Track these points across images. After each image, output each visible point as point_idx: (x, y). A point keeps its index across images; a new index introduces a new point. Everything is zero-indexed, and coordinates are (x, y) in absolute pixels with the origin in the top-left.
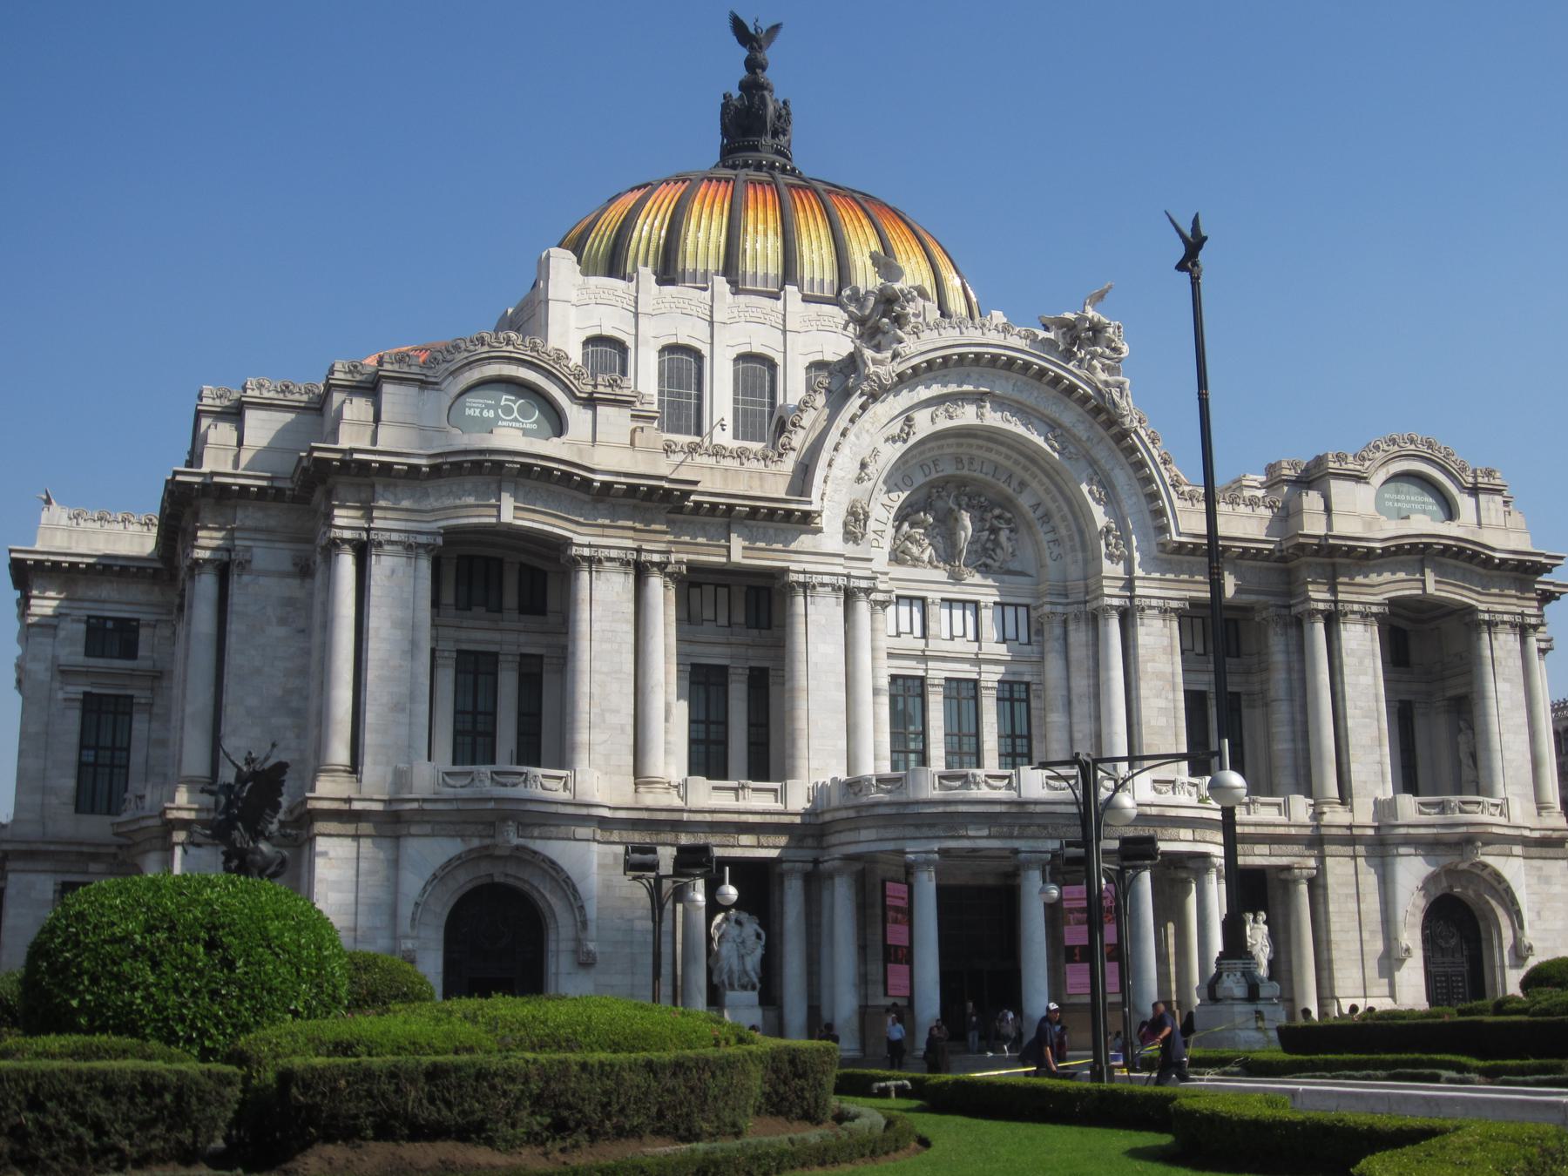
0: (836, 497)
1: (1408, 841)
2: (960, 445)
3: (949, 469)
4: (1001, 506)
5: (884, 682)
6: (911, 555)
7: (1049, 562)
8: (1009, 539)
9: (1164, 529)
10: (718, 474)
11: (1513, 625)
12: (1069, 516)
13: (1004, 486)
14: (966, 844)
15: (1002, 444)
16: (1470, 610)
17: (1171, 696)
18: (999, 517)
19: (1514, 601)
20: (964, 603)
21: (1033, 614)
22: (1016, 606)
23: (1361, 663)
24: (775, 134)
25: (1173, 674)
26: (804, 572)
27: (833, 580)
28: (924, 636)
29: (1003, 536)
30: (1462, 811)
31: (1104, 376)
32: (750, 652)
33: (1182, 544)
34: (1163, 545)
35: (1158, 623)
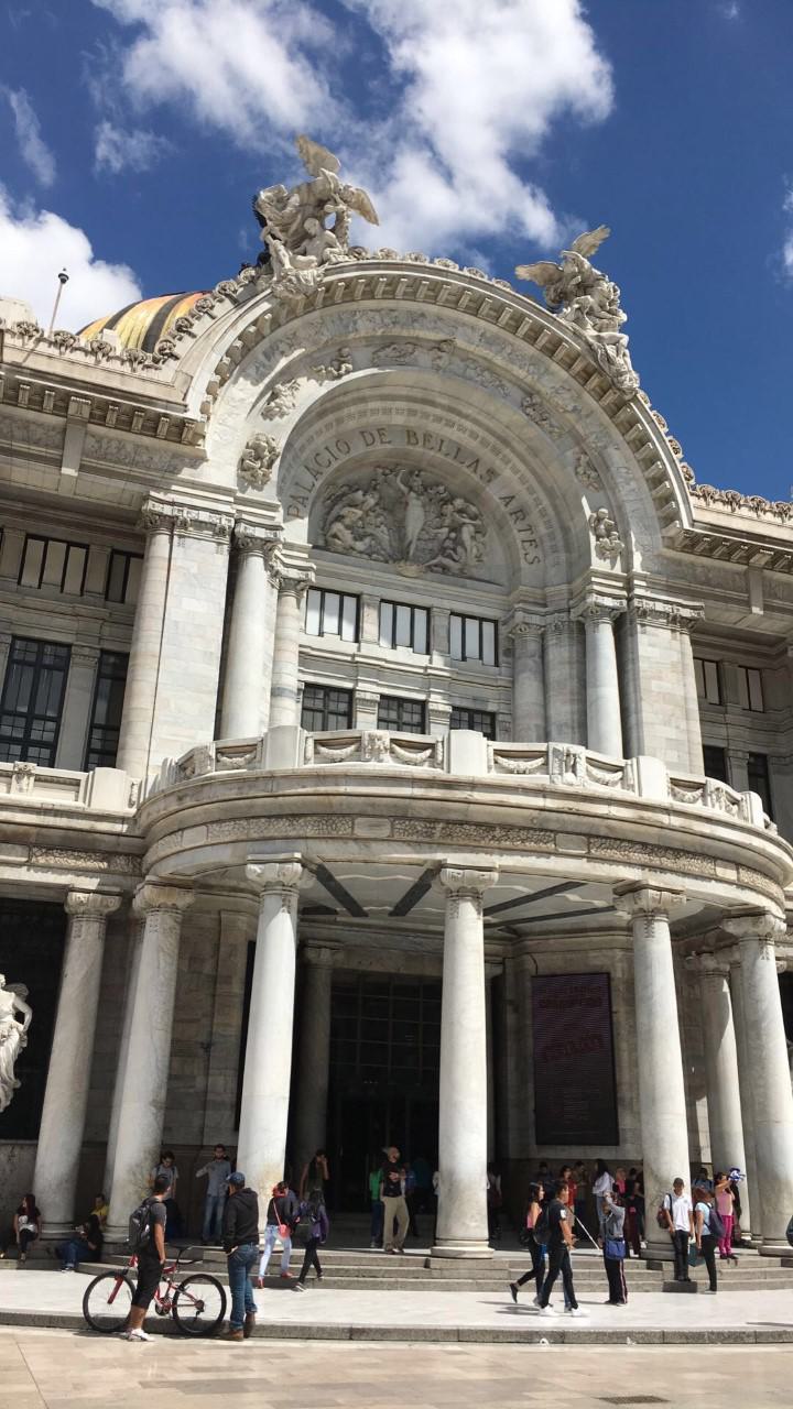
0: (230, 421)
2: (412, 413)
4: (466, 501)
5: (292, 678)
7: (523, 564)
8: (473, 538)
9: (675, 516)
12: (551, 511)
15: (466, 417)
17: (683, 725)
18: (460, 511)
21: (503, 630)
22: (482, 620)
25: (686, 699)
26: (172, 504)
27: (215, 519)
28: (357, 640)
29: (467, 533)
32: (107, 630)
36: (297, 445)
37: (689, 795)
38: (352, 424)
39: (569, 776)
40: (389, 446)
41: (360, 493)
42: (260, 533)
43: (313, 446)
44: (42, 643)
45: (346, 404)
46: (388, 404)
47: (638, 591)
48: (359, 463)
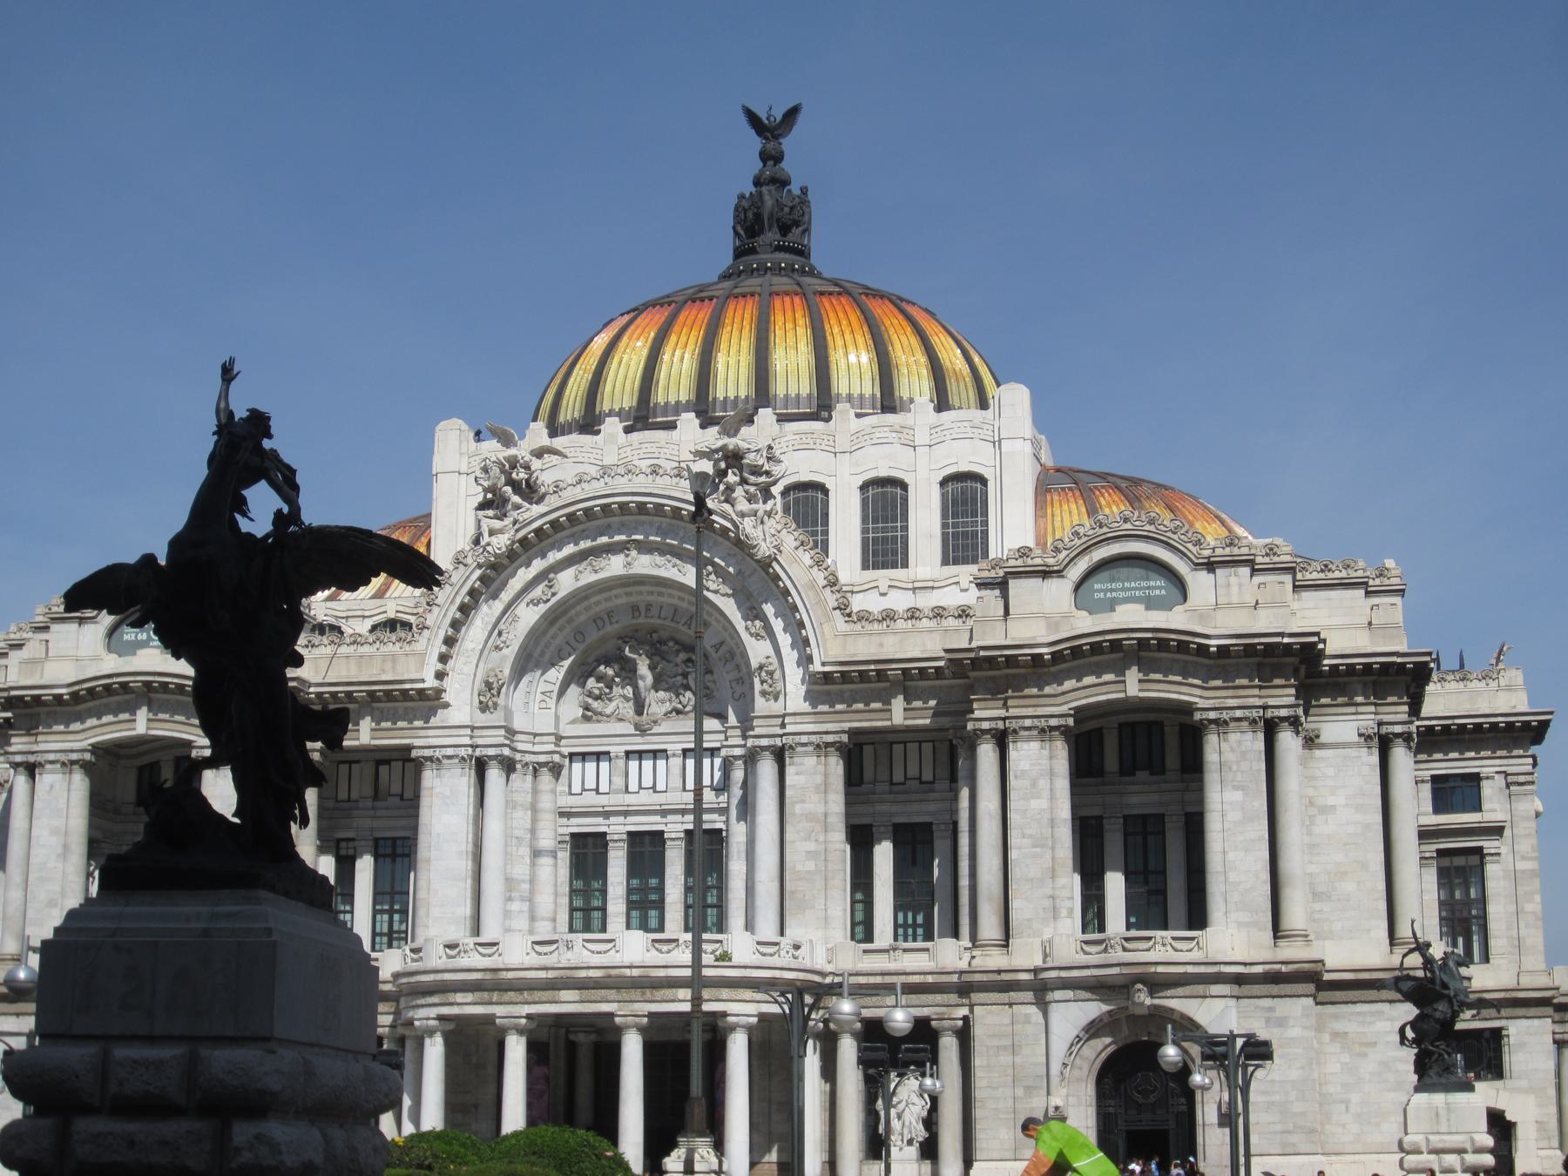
1: (1065, 984)
2: (628, 594)
3: (624, 622)
5: (546, 841)
6: (596, 713)
9: (810, 659)
10: (353, 662)
11: (1254, 722)
13: (684, 629)
14: (455, 1010)
16: (1187, 709)
17: (821, 838)
19: (1256, 692)
20: (655, 754)
23: (1034, 785)
24: (785, 229)
25: (826, 815)
30: (1125, 950)
31: (743, 505)
33: (826, 674)
34: (813, 675)
35: (810, 761)
36: (536, 654)
37: (665, 948)
38: (582, 618)
39: (569, 955)
40: (616, 626)
41: (602, 668)
42: (491, 752)
43: (552, 648)
44: (394, 840)
45: (573, 606)
46: (605, 595)
47: (789, 729)
48: (603, 640)
